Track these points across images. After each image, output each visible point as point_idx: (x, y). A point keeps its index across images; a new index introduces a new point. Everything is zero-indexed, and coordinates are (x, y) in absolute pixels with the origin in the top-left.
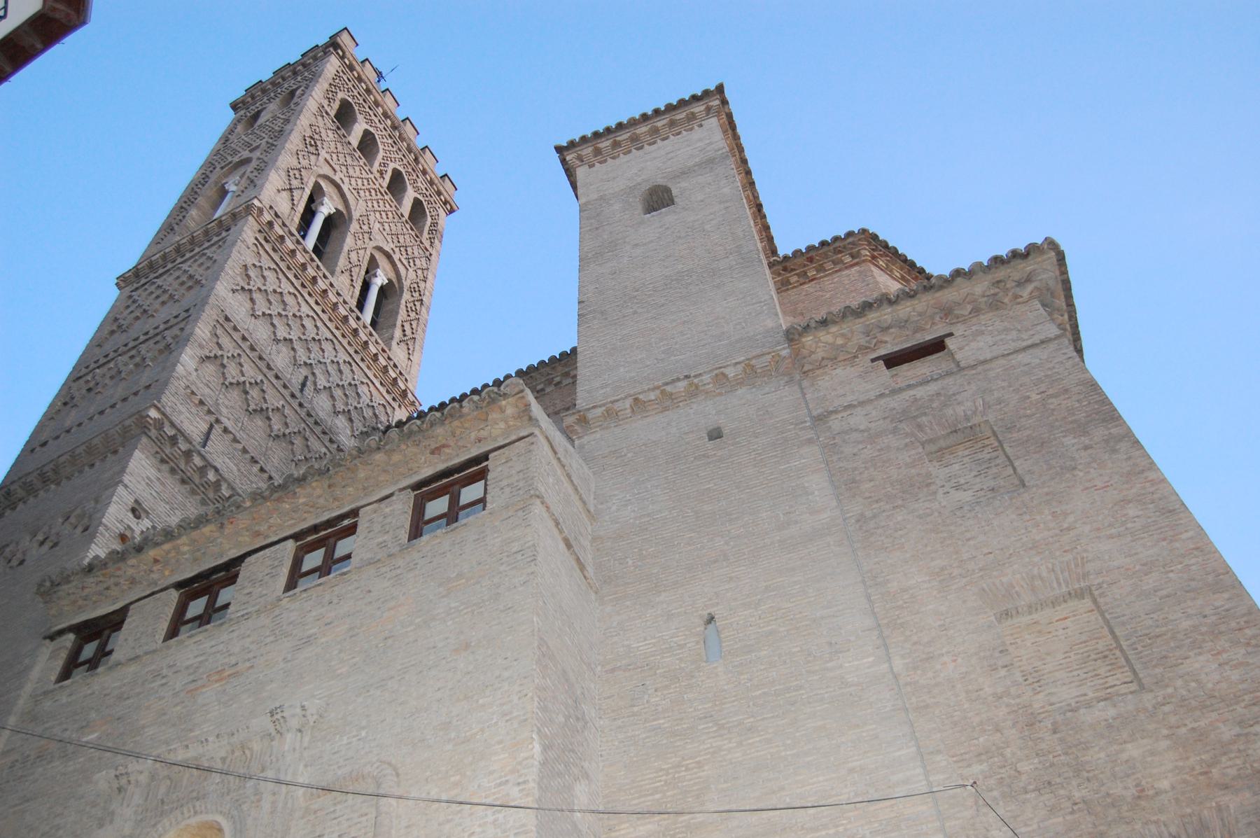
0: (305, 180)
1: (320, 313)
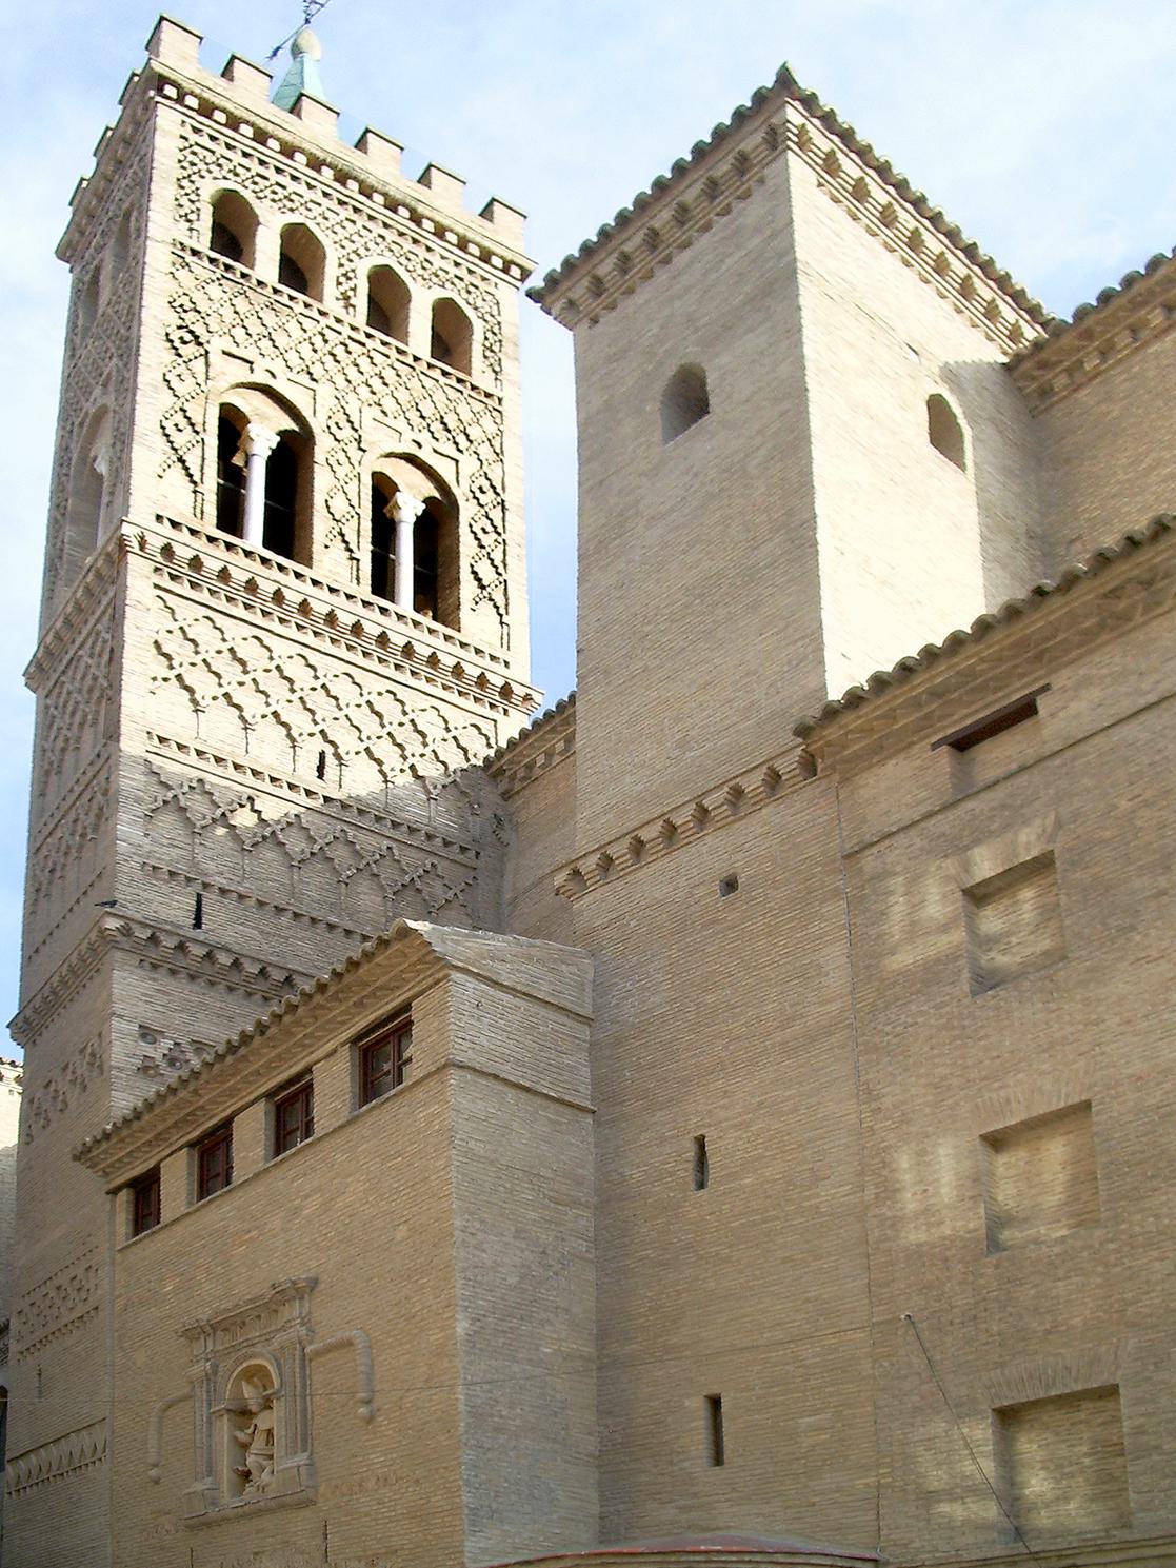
0: (197, 419)
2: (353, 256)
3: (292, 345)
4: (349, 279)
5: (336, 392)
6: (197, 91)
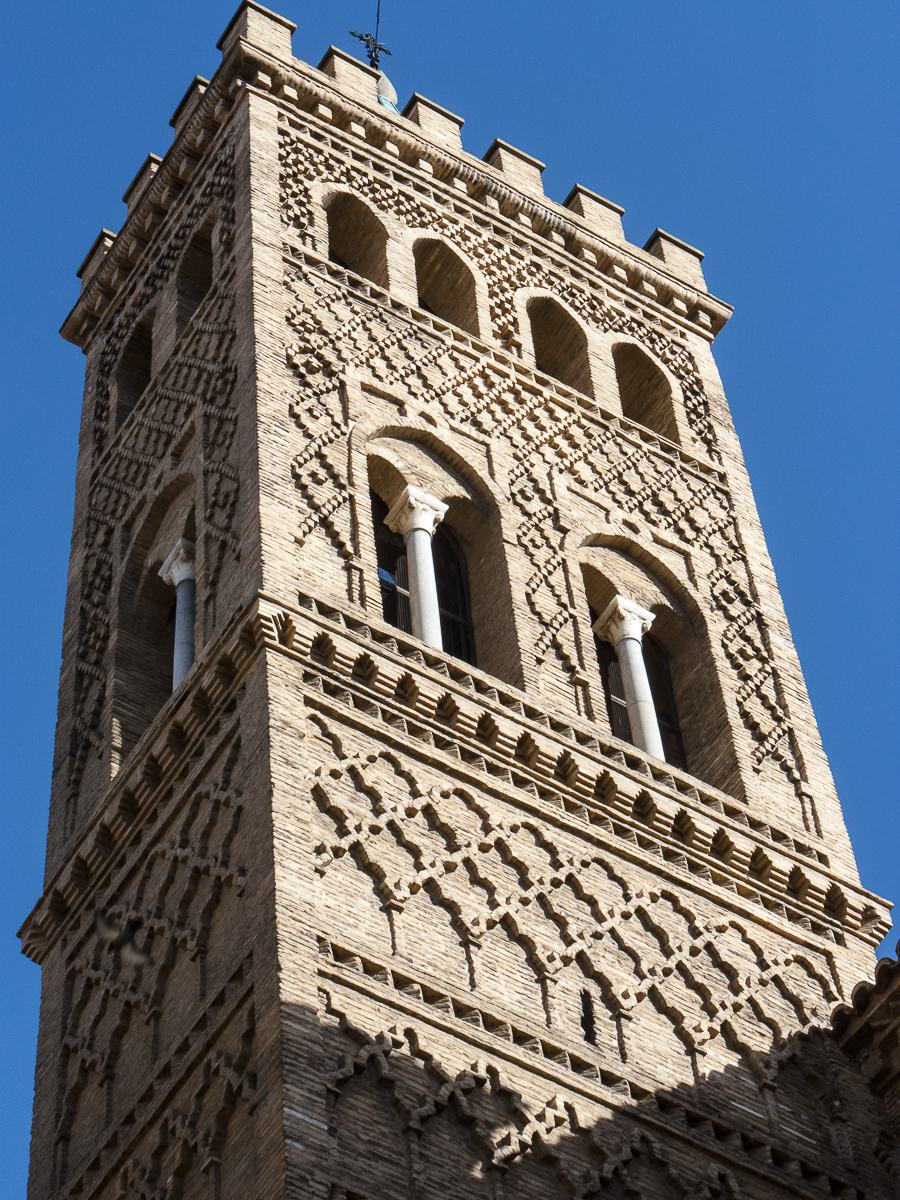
0: (341, 469)
1: (536, 802)
2: (506, 285)
3: (449, 385)
4: (505, 311)
5: (514, 450)
6: (298, 79)
